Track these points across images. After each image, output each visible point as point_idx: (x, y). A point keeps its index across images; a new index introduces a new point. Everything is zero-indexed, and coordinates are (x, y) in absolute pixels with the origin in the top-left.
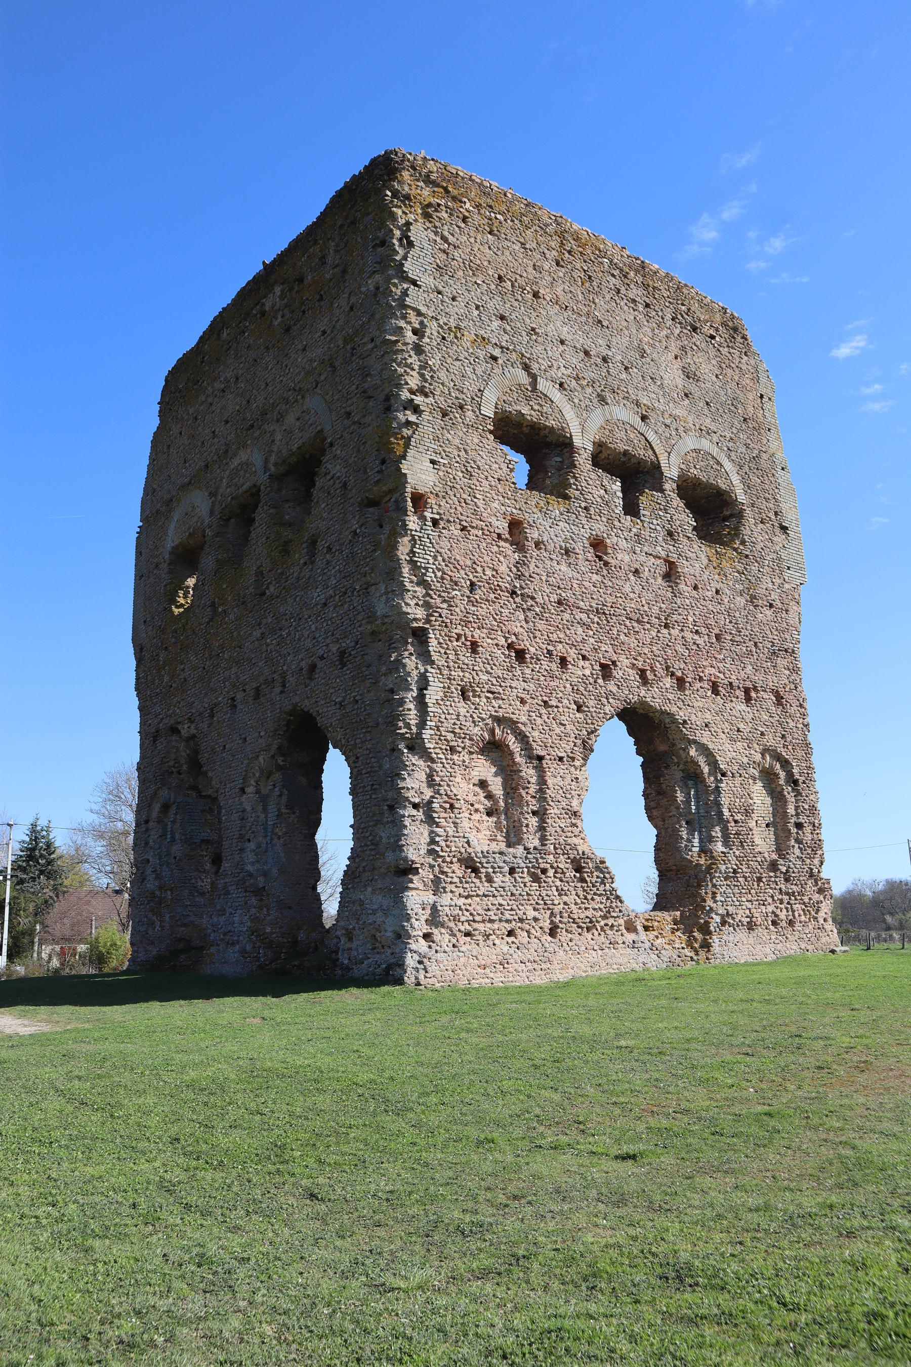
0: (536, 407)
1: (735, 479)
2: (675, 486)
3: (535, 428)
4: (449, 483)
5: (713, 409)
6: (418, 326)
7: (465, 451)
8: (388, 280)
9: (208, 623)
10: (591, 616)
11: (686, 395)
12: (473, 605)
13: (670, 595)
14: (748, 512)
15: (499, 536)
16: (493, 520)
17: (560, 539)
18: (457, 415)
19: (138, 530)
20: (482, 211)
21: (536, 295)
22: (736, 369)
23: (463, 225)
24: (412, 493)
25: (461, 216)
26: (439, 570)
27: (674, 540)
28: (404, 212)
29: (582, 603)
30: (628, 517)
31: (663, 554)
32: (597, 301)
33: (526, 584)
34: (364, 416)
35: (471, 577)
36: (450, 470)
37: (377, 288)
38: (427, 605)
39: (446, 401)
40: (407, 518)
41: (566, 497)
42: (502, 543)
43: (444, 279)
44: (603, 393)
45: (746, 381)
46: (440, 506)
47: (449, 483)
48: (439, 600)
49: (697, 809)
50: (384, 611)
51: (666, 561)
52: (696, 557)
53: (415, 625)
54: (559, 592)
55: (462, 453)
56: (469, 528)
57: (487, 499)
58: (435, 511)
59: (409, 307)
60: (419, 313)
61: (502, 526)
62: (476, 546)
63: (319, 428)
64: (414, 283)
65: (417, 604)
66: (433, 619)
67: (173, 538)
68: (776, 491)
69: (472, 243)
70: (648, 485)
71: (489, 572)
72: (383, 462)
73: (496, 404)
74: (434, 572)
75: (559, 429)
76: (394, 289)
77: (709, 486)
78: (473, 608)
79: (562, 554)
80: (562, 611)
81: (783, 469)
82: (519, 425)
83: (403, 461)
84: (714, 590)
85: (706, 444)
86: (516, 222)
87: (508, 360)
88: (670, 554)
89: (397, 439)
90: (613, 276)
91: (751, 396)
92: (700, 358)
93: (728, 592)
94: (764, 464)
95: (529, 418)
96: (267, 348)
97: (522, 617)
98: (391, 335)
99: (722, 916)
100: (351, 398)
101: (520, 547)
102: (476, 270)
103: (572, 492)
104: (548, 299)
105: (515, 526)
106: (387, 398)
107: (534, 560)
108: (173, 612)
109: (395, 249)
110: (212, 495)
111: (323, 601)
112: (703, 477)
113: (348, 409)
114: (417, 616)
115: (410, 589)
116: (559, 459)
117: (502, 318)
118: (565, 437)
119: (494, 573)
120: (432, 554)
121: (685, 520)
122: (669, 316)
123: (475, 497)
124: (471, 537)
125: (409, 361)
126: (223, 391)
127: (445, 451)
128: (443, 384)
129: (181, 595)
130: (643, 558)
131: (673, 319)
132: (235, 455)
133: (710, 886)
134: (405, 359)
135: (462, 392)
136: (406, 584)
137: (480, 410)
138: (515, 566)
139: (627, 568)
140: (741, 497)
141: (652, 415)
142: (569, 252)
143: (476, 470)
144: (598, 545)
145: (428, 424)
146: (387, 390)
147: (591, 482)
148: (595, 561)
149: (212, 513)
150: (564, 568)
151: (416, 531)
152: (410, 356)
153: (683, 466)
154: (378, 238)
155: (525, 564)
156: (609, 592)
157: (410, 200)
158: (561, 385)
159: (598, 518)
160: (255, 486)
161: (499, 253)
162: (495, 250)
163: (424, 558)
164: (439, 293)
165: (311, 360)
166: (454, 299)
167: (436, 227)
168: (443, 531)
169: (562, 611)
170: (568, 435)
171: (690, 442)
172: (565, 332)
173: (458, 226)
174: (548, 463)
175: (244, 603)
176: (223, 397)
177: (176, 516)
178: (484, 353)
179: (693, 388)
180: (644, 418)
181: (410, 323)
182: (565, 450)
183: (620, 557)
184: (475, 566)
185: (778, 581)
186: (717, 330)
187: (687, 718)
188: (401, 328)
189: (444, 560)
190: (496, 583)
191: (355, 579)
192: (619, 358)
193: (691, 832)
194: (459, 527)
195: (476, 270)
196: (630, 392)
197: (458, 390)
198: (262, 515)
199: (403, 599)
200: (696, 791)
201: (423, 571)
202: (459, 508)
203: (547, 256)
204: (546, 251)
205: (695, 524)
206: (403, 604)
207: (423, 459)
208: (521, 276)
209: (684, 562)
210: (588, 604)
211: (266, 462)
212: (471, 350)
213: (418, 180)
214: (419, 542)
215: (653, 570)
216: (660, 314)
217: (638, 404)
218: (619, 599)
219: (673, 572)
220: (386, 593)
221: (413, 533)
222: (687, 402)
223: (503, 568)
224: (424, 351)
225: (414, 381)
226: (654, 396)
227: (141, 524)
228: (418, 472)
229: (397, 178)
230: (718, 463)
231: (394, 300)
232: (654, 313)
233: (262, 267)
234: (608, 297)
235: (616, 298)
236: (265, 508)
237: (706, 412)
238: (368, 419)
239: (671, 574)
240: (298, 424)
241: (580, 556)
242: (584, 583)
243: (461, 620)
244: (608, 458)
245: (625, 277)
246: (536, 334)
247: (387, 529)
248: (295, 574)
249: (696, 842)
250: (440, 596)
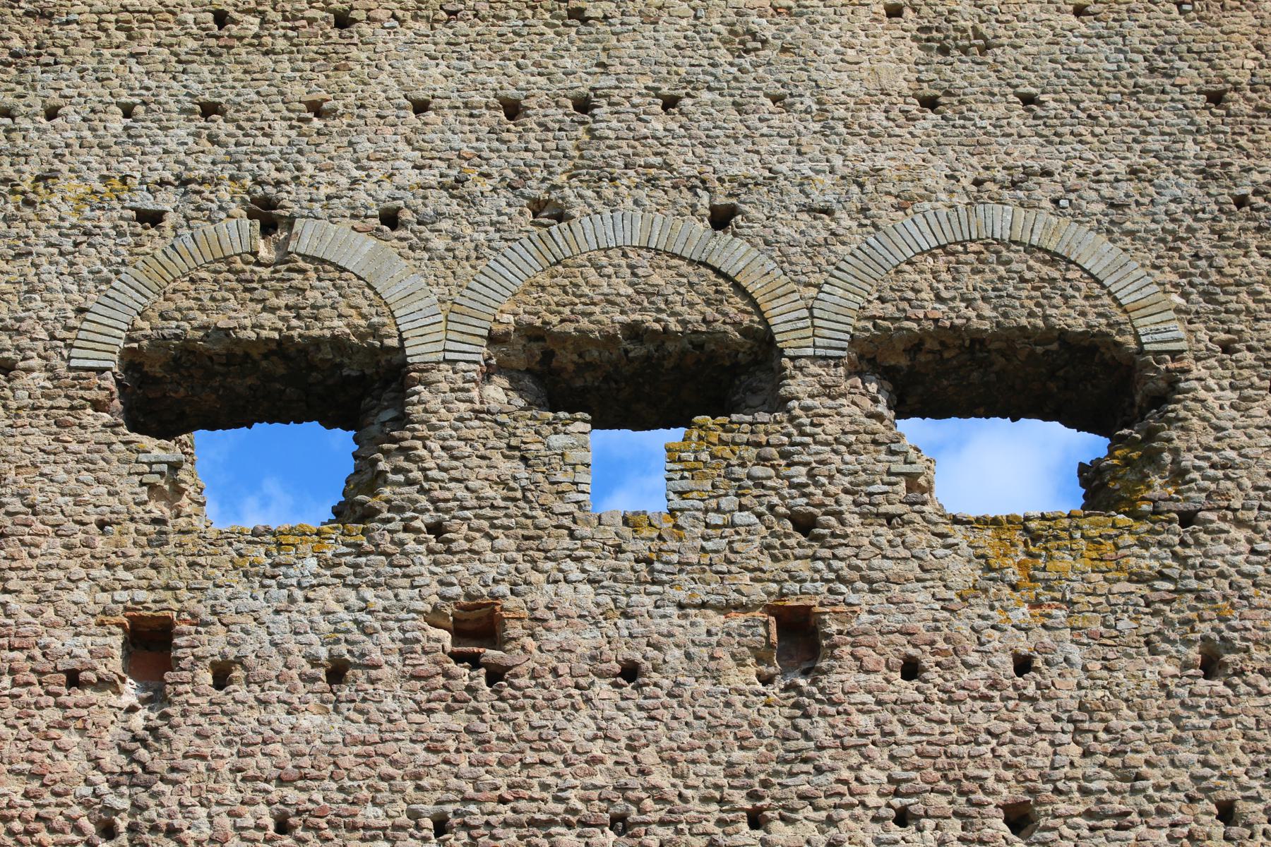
31: (757, 593)
57: (50, 587)
75: (362, 337)
77: (1010, 340)
85: (1002, 219)
93: (1076, 654)
112: (983, 317)
172: (434, 79)
179: (963, 73)
180: (721, 219)
230: (1054, 258)
246: (332, 113)
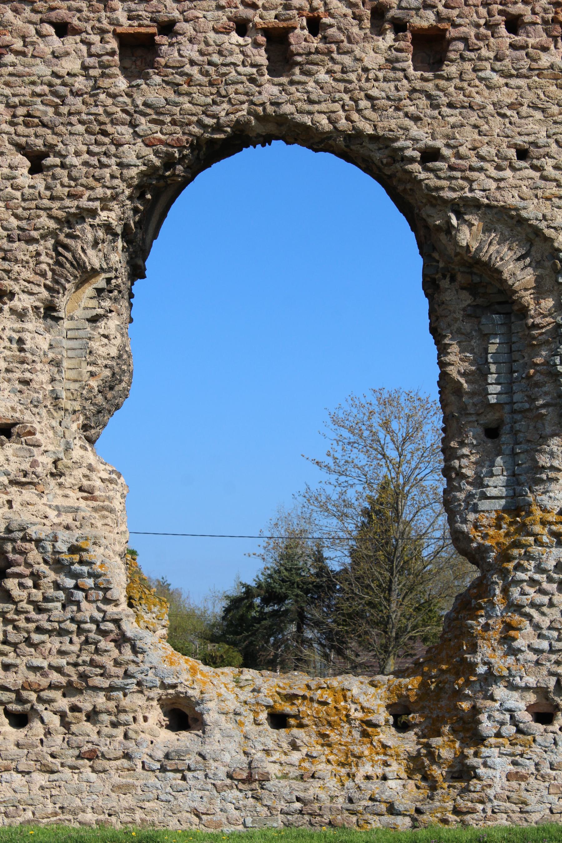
49: (508, 391)
99: (541, 691)
133: (499, 608)
187: (439, 143)
193: (485, 462)
200: (508, 343)
249: (497, 485)
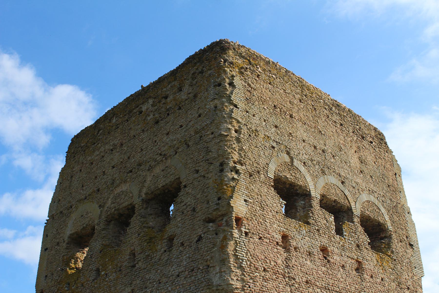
0: (293, 174)
1: (387, 217)
2: (359, 220)
3: (292, 185)
4: (253, 213)
5: (374, 180)
6: (237, 128)
7: (261, 195)
8: (223, 104)
9: (93, 280)
10: (323, 291)
11: (361, 172)
12: (266, 282)
13: (360, 280)
14: (394, 236)
15: (277, 243)
16: (274, 234)
17: (306, 246)
18: (257, 177)
19: (46, 222)
20: (266, 73)
21: (291, 116)
22: (383, 159)
23: (257, 79)
24: (236, 217)
25: (256, 74)
26: (249, 260)
27: (360, 249)
28: (230, 71)
29: (318, 283)
30: (338, 236)
31: (356, 257)
32: (319, 121)
33: (291, 271)
34: (208, 173)
35: (264, 266)
36: (253, 206)
37: (216, 107)
38: (243, 280)
39: (251, 169)
40: (233, 231)
41: (308, 223)
42: (278, 247)
43: (250, 106)
44: (324, 169)
45: (388, 166)
46: (249, 225)
47: (253, 213)
48: (249, 278)
50: (218, 283)
51: (357, 261)
52: (370, 259)
53: (236, 291)
54: (307, 276)
55: (259, 197)
56: (263, 238)
57: (271, 223)
58: (247, 228)
59: (233, 118)
60: (238, 122)
61: (278, 238)
62: (266, 248)
63: (177, 177)
64: (236, 106)
65: (237, 280)
66: (246, 288)
67: (70, 229)
68: (406, 225)
69: (262, 88)
70: (345, 219)
71: (273, 263)
72: (219, 199)
73: (275, 171)
74: (246, 262)
75: (304, 187)
76: (226, 108)
78: (266, 284)
79: (307, 255)
80: (308, 287)
81: (408, 213)
82: (285, 183)
83: (231, 200)
84: (380, 278)
85: (372, 198)
86: (281, 79)
87: (280, 149)
88: (359, 257)
89: (228, 187)
90: (326, 109)
91: (391, 174)
92: (366, 153)
93: (387, 280)
94: (399, 210)
95: (290, 180)
96: (143, 131)
97: (289, 290)
98: (224, 132)
100: (199, 163)
101: (287, 249)
102: (264, 102)
103: (311, 221)
104: (297, 119)
105: (285, 237)
106: (222, 164)
107: (294, 258)
108: (67, 272)
109: (226, 89)
110: (100, 206)
111: (177, 273)
113: (197, 168)
114: (238, 286)
115: (234, 270)
116: (303, 202)
117: (276, 127)
118: (307, 191)
119: (275, 264)
120: (245, 251)
121: (365, 239)
122: (351, 131)
123: (266, 221)
124: (264, 243)
125: (234, 146)
126: (112, 150)
127: (251, 195)
128: (250, 159)
129: (73, 262)
130: (346, 259)
131: (353, 132)
132: (118, 186)
134: (232, 145)
135: (259, 164)
136: (232, 267)
137: (267, 174)
138: (286, 261)
139: (339, 264)
140: (390, 228)
141: (346, 181)
142: (306, 96)
143: (266, 207)
144: (324, 250)
145: (243, 180)
146: (222, 160)
147: (320, 216)
148: (323, 260)
149: (100, 217)
150: (308, 263)
151: (237, 238)
152: (234, 143)
153: (362, 210)
154: (217, 82)
155: (290, 260)
156: (330, 277)
157: (233, 65)
158: (304, 163)
159: (324, 236)
160: (131, 204)
161: (274, 94)
162: (272, 92)
163: (242, 254)
164: (247, 112)
165: (172, 140)
166: (254, 115)
167: (245, 79)
168: (251, 239)
169: (308, 287)
170: (308, 190)
171: (365, 197)
173: (255, 79)
174: (297, 204)
175: (120, 270)
176: (112, 153)
177: (74, 216)
178: (269, 144)
180: (343, 183)
181: (234, 126)
182: (306, 198)
183: (335, 257)
184: (266, 259)
185: (410, 275)
186: (373, 139)
188: (229, 129)
189: (251, 255)
190: (276, 270)
191: (200, 262)
192: (330, 151)
194: (258, 237)
195: (264, 102)
196: (336, 169)
197: (257, 163)
198: (135, 221)
199: (230, 276)
201: (241, 261)
202: (258, 227)
203: (296, 97)
204: (295, 95)
205: (370, 241)
206: (230, 279)
207: (241, 199)
208: (284, 106)
209: (366, 262)
210: (320, 283)
211: (140, 192)
212: (262, 143)
213: (236, 55)
214: (239, 244)
215: (351, 266)
216: (347, 129)
217: (340, 176)
218: (336, 282)
219: (360, 267)
220: (221, 272)
221: (236, 239)
222: (362, 175)
223: (279, 262)
224: (241, 142)
225: (236, 157)
226: (346, 171)
227: (48, 218)
228: (239, 206)
229: (226, 53)
230: (378, 208)
231: (226, 114)
232: (345, 129)
233: (141, 88)
234: (323, 120)
235: (327, 120)
236: (139, 217)
237: (371, 181)
238: (210, 175)
239: (359, 268)
240: (162, 173)
241: (316, 257)
242: (319, 272)
243: (259, 290)
244: (326, 203)
245: (331, 110)
246: (292, 136)
247: (221, 236)
248: (158, 257)
250: (249, 275)
